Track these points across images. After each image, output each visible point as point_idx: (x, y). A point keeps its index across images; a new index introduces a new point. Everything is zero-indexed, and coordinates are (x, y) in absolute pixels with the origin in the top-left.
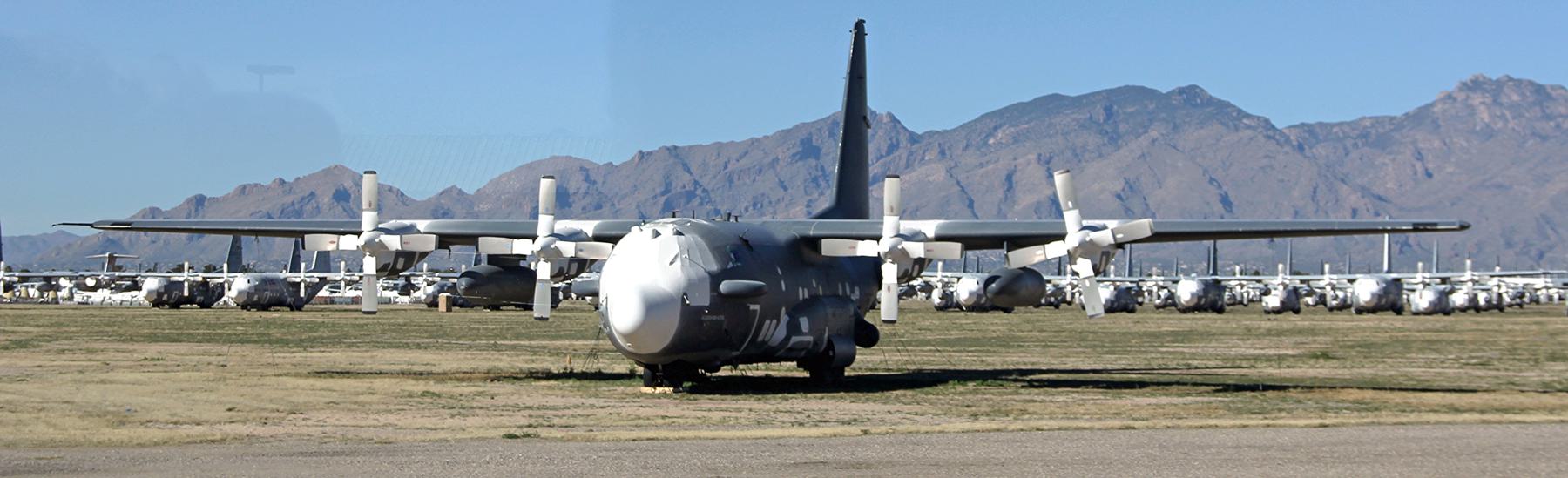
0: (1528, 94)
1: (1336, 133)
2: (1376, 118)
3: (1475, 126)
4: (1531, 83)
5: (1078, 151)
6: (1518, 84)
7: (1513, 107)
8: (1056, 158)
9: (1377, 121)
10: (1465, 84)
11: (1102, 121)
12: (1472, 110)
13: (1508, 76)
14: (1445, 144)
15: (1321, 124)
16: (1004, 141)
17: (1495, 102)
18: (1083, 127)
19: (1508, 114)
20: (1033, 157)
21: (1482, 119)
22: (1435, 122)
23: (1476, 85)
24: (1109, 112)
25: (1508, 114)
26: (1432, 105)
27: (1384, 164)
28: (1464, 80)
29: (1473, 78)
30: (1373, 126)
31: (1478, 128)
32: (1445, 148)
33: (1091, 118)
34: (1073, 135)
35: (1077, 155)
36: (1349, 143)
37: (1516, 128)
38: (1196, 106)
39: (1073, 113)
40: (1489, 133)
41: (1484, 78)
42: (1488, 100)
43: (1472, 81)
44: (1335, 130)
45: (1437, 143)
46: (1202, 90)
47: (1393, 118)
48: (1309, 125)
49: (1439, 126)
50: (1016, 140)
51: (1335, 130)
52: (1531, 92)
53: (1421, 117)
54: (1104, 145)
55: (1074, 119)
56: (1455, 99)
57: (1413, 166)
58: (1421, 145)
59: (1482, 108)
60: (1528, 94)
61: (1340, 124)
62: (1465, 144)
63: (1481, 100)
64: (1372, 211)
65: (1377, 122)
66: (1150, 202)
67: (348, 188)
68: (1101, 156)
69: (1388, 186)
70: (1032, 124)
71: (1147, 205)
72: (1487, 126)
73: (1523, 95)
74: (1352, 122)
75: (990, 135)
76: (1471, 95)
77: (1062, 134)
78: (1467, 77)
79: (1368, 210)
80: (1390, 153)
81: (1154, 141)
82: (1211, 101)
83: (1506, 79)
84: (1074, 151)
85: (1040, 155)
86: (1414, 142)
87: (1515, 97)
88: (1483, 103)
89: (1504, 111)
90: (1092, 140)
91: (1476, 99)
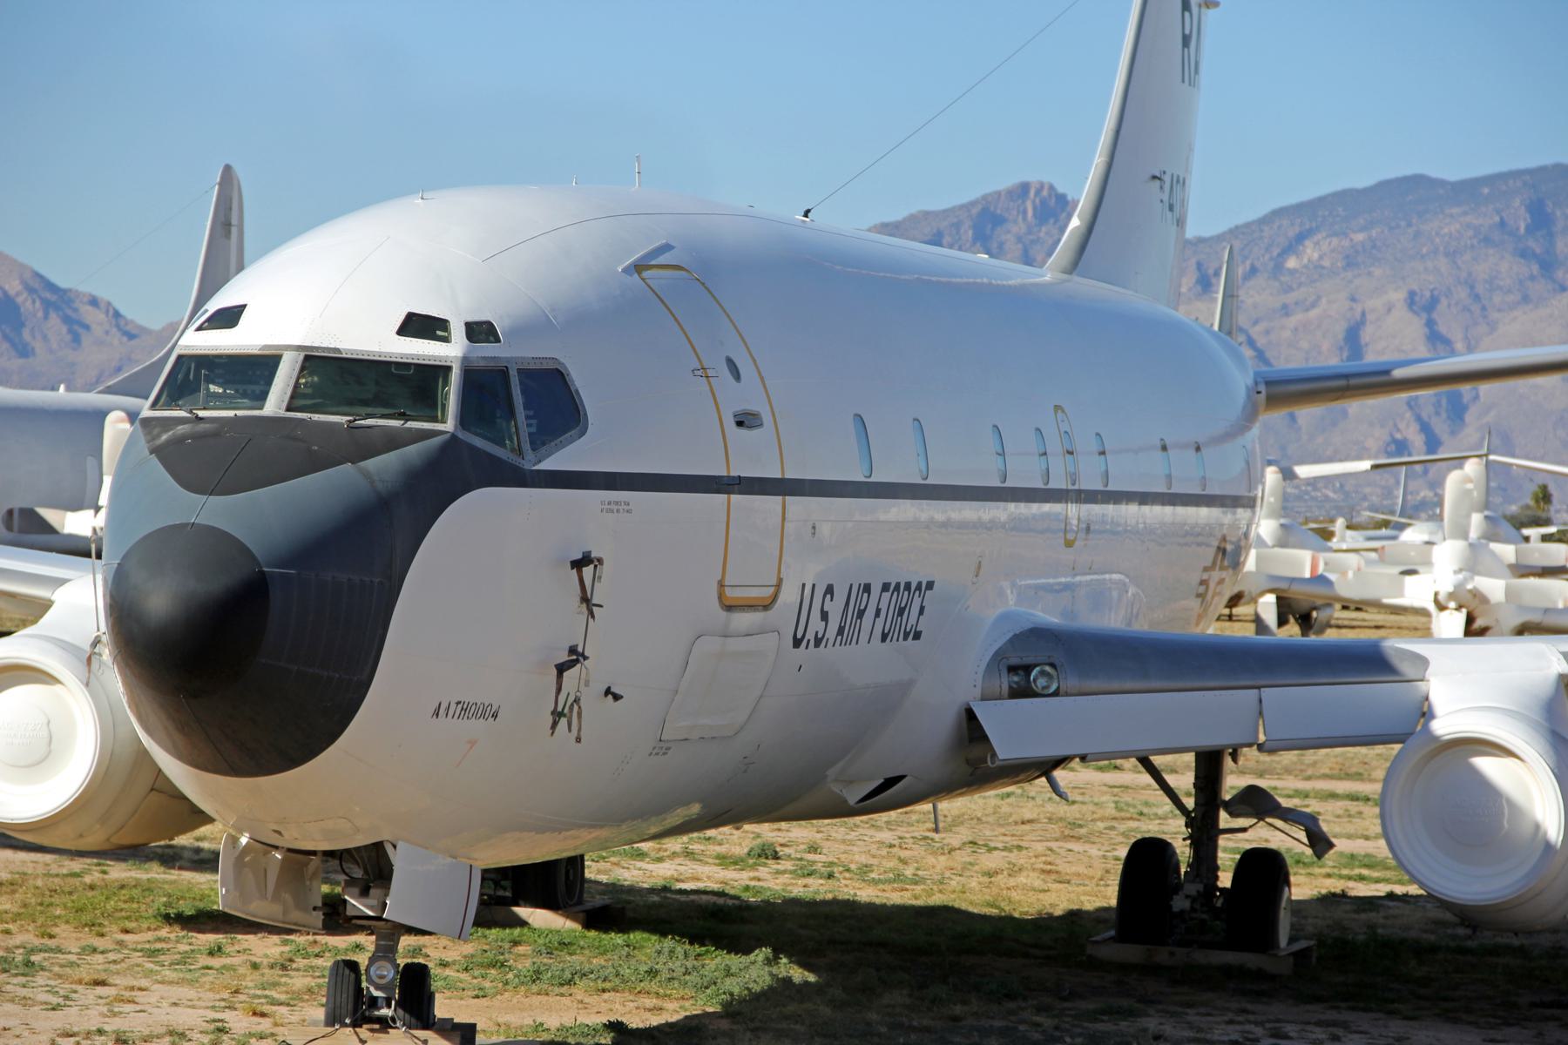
5: (1480, 289)
8: (1444, 302)
11: (1522, 230)
16: (1326, 263)
18: (1487, 241)
20: (1398, 296)
24: (1541, 219)
33: (1502, 223)
35: (1477, 297)
39: (1465, 213)
50: (1350, 263)
54: (1532, 278)
67: (12, 292)
68: (1526, 299)
70: (1374, 233)
77: (1447, 255)
84: (1472, 287)
85: (1412, 294)
90: (1505, 267)
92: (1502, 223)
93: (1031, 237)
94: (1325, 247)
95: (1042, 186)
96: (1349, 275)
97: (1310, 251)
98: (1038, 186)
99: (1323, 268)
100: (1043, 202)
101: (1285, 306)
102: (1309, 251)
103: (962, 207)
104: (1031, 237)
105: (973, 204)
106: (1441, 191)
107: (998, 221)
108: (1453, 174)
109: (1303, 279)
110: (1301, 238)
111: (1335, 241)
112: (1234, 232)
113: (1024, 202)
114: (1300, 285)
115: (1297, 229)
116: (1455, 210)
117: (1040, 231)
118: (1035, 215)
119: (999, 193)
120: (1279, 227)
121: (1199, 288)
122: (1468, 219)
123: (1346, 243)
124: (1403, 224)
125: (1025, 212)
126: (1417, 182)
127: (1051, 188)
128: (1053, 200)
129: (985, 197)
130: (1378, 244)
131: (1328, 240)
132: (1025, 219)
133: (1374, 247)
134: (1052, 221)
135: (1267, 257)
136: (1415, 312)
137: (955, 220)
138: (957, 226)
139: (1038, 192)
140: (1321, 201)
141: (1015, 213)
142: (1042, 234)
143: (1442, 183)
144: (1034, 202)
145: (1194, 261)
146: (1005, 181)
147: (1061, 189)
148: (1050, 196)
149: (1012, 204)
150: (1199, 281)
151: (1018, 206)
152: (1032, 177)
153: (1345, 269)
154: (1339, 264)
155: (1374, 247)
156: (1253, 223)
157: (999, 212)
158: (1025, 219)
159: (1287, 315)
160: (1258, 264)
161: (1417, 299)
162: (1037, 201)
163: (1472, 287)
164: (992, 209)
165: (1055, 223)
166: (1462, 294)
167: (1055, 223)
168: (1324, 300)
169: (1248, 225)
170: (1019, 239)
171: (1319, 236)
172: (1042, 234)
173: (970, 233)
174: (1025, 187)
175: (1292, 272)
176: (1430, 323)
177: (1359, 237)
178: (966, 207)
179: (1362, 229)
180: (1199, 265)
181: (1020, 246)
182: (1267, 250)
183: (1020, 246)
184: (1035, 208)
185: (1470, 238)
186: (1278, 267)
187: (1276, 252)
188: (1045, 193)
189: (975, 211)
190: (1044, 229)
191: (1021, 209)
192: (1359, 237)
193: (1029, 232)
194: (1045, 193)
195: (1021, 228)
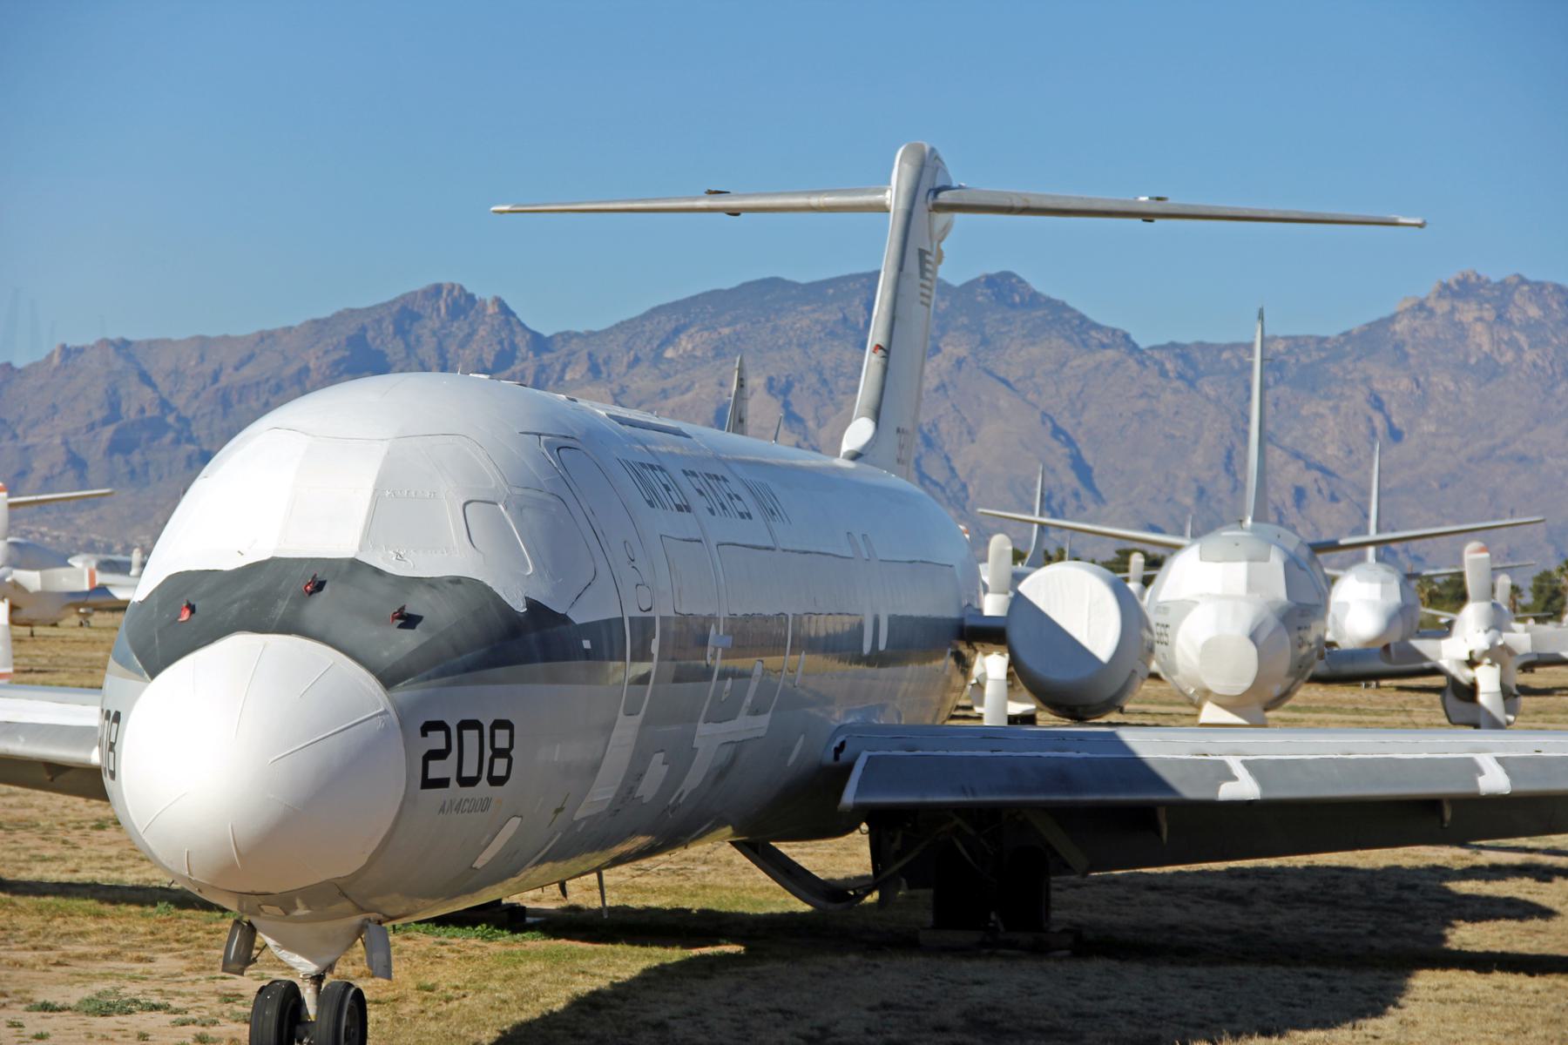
5: (827, 375)
8: (797, 386)
16: (698, 353)
18: (832, 334)
22: (1399, 346)
27: (1322, 416)
30: (1289, 351)
32: (1419, 392)
33: (845, 319)
34: (817, 347)
35: (825, 382)
38: (1013, 306)
39: (814, 311)
45: (1405, 384)
46: (1021, 281)
47: (1322, 340)
48: (1183, 347)
49: (1406, 356)
55: (817, 321)
57: (1370, 420)
58: (1377, 386)
62: (1452, 386)
64: (1326, 492)
66: (957, 465)
69: (1329, 452)
70: (738, 327)
71: (952, 470)
75: (670, 339)
77: (799, 345)
79: (1320, 491)
80: (1327, 397)
81: (959, 363)
82: (1035, 300)
84: (820, 374)
85: (771, 380)
86: (1367, 380)
92: (845, 319)
93: (444, 331)
94: (698, 339)
95: (453, 286)
96: (718, 363)
97: (685, 343)
98: (450, 287)
99: (695, 357)
100: (455, 301)
101: (664, 391)
102: (684, 343)
103: (383, 305)
104: (444, 331)
105: (393, 303)
106: (794, 292)
107: (416, 317)
108: (804, 279)
109: (679, 367)
110: (677, 331)
111: (706, 334)
112: (621, 326)
113: (437, 301)
114: (676, 372)
115: (673, 324)
116: (806, 308)
117: (452, 326)
119: (415, 293)
120: (659, 323)
121: (590, 374)
122: (816, 315)
123: (715, 336)
124: (763, 320)
125: (438, 310)
126: (773, 283)
127: (461, 288)
129: (403, 297)
130: (742, 336)
131: (700, 334)
132: (439, 315)
133: (738, 339)
134: (462, 317)
135: (648, 348)
136: (775, 396)
137: (377, 317)
138: (379, 321)
139: (450, 292)
140: (694, 300)
141: (429, 310)
142: (453, 329)
143: (795, 285)
144: (446, 300)
145: (585, 352)
147: (469, 290)
148: (460, 296)
149: (426, 303)
150: (589, 370)
151: (433, 305)
152: (444, 279)
153: (716, 356)
154: (710, 354)
155: (738, 339)
156: (636, 318)
157: (416, 309)
159: (666, 398)
160: (640, 355)
161: (775, 383)
162: (449, 300)
163: (820, 374)
164: (410, 307)
165: (465, 318)
166: (812, 379)
167: (465, 318)
168: (697, 386)
169: (631, 321)
170: (434, 333)
171: (693, 330)
172: (453, 329)
173: (391, 328)
174: (438, 289)
175: (671, 360)
176: (786, 405)
177: (726, 331)
179: (728, 325)
180: (590, 355)
181: (435, 339)
182: (649, 341)
183: (435, 339)
184: (447, 306)
185: (819, 332)
186: (658, 357)
187: (656, 343)
188: (456, 293)
189: (395, 309)
190: (455, 324)
191: (436, 306)
192: (726, 331)
193: (443, 327)
194: (456, 293)
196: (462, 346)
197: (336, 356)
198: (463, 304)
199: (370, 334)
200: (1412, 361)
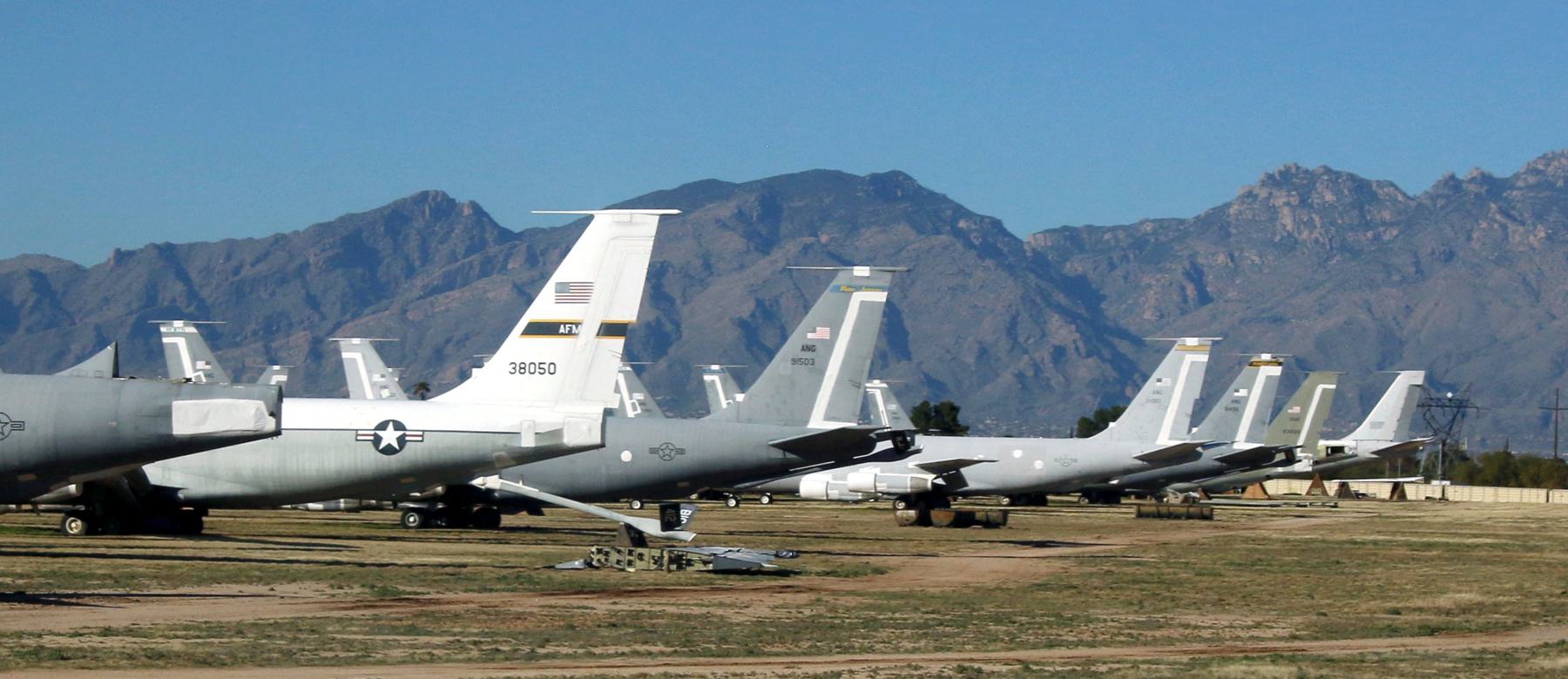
0: (1346, 192)
1: (1108, 241)
2: (1163, 220)
3: (1274, 234)
4: (1352, 177)
6: (1333, 176)
7: (1325, 210)
9: (1162, 225)
10: (1270, 177)
12: (1273, 212)
13: (1325, 167)
14: (1232, 260)
15: (1090, 229)
17: (1304, 202)
19: (1316, 218)
21: (1284, 226)
23: (1283, 179)
25: (1316, 218)
26: (1228, 205)
28: (1271, 173)
29: (1283, 169)
30: (1155, 232)
31: (1277, 239)
36: (1116, 256)
37: (1321, 239)
40: (1289, 245)
41: (1298, 168)
42: (1294, 200)
43: (1281, 173)
44: (1107, 237)
45: (1221, 259)
47: (1182, 222)
49: (1229, 235)
51: (1107, 237)
52: (1349, 191)
53: (1215, 223)
56: (1256, 197)
59: (1286, 210)
60: (1346, 192)
61: (1113, 229)
62: (1257, 260)
63: (1285, 200)
65: (1161, 227)
72: (1290, 235)
73: (1338, 193)
74: (1129, 226)
76: (1275, 192)
78: (1275, 167)
83: (1321, 170)
87: (1329, 197)
88: (1288, 204)
89: (1313, 216)
91: (1280, 199)
95: (437, 193)
118: (431, 215)
119: (405, 200)
127: (444, 194)
128: (445, 203)
129: (395, 203)
132: (423, 217)
142: (437, 229)
144: (430, 205)
146: (407, 188)
147: (451, 196)
148: (442, 200)
152: (430, 187)
158: (423, 217)
172: (437, 229)
174: (424, 196)
178: (380, 210)
188: (439, 199)
189: (386, 213)
194: (439, 199)
195: (419, 223)
196: (441, 243)
197: (330, 253)
198: (443, 207)
199: (365, 234)
200: (1232, 240)
